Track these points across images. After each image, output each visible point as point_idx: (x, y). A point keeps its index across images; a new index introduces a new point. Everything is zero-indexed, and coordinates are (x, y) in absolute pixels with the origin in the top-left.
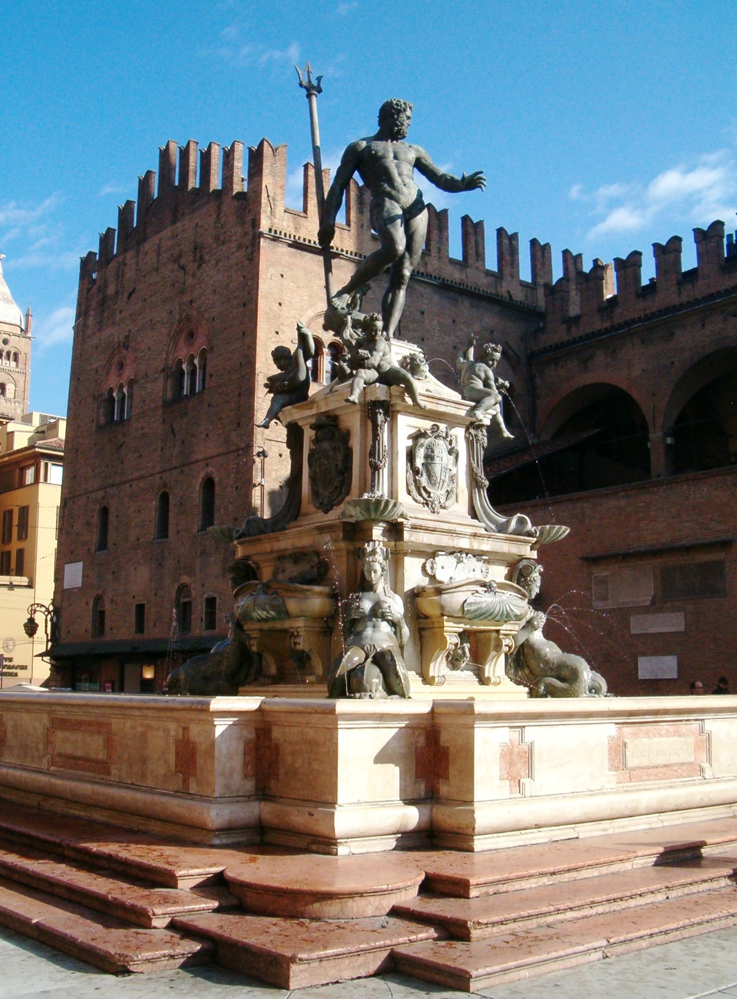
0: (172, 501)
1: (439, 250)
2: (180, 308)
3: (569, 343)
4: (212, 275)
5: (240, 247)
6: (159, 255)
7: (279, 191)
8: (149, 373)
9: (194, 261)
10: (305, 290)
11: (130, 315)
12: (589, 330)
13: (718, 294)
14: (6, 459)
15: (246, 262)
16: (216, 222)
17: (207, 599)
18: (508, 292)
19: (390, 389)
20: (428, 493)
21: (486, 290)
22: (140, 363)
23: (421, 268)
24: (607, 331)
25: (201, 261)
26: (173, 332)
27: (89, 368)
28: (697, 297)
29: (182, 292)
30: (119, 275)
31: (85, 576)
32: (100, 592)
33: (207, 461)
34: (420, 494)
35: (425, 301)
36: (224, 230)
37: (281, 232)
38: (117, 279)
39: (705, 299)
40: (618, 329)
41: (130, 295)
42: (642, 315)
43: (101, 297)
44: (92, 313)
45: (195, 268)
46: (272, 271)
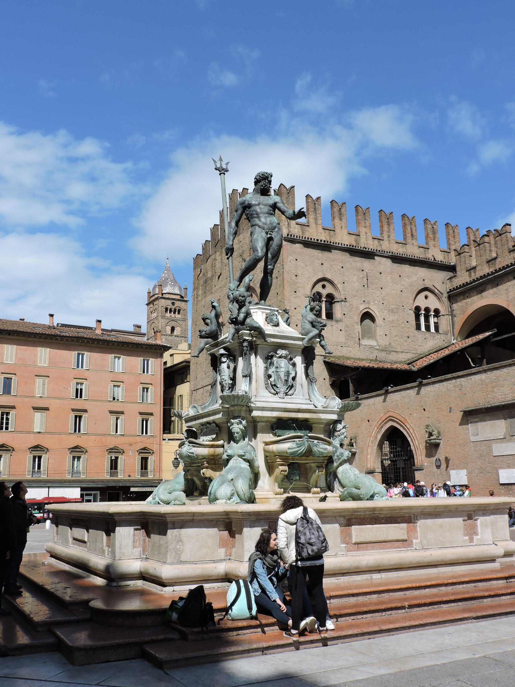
1: (389, 236)
3: (471, 283)
10: (310, 266)
11: (220, 287)
12: (482, 274)
14: (170, 370)
18: (433, 256)
20: (278, 387)
21: (418, 256)
23: (378, 247)
24: (492, 273)
30: (213, 266)
35: (382, 266)
37: (294, 236)
40: (499, 271)
41: (219, 277)
44: (201, 287)
46: (290, 258)
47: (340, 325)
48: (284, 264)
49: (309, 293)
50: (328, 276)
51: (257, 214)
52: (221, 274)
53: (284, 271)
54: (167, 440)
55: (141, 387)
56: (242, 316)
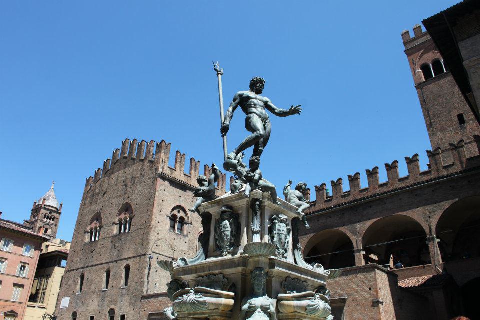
0: (112, 274)
1: (222, 188)
4: (138, 188)
5: (149, 179)
6: (118, 179)
7: (166, 160)
13: (324, 210)
15: (152, 184)
16: (142, 169)
17: (121, 315)
25: (135, 183)
27: (84, 220)
29: (125, 194)
30: (101, 186)
31: (71, 303)
32: (76, 310)
33: (128, 259)
38: (100, 188)
39: (319, 211)
46: (161, 188)
47: (185, 239)
49: (169, 214)
50: (183, 205)
51: (255, 105)
54: (37, 307)
55: (21, 265)
56: (257, 176)
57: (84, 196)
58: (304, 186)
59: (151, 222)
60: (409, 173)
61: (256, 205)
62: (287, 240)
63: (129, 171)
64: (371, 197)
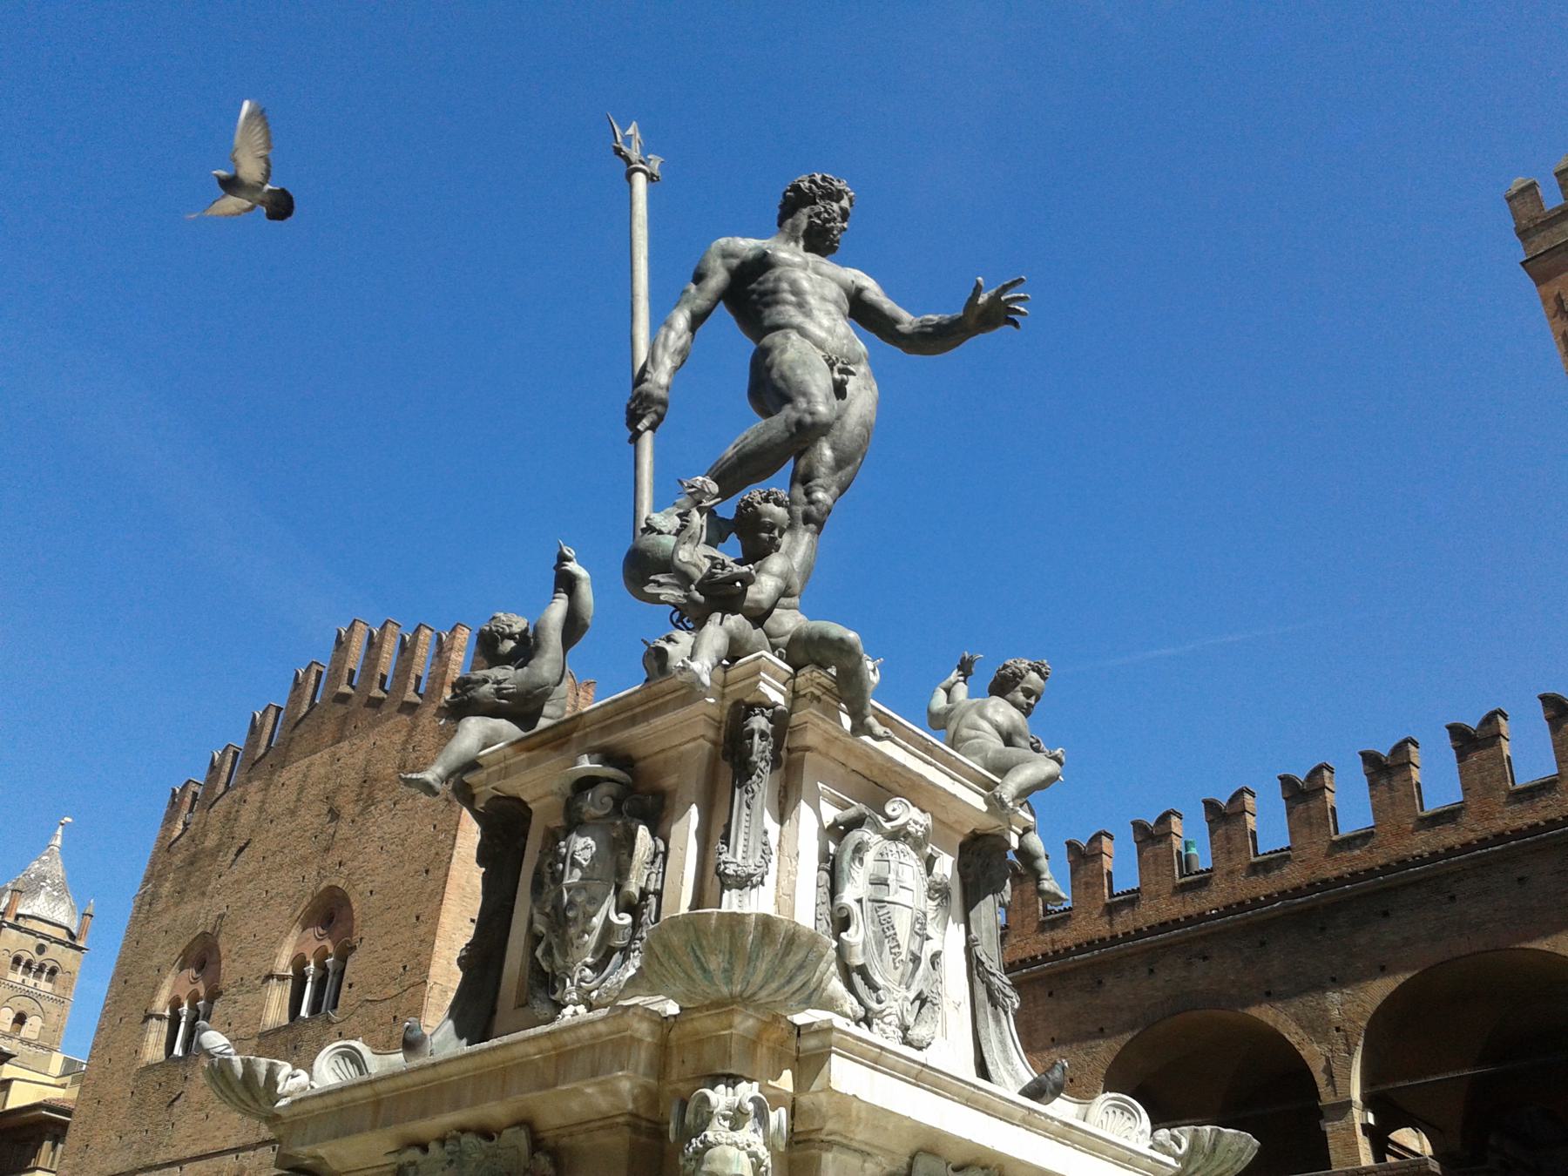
2: (319, 873)
4: (384, 823)
8: (245, 977)
9: (357, 800)
16: (406, 742)
19: (794, 676)
20: (874, 988)
22: (234, 961)
25: (371, 801)
26: (298, 913)
28: (1139, 925)
29: (327, 850)
30: (230, 818)
34: (851, 988)
36: (413, 756)
39: (1153, 930)
42: (1049, 949)
43: (193, 850)
45: (358, 809)
48: (460, 834)
52: (247, 844)
53: (455, 853)
57: (153, 864)
58: (1034, 676)
59: (429, 966)
60: (1560, 762)
61: (751, 734)
62: (929, 949)
63: (355, 753)
64: (1386, 869)
